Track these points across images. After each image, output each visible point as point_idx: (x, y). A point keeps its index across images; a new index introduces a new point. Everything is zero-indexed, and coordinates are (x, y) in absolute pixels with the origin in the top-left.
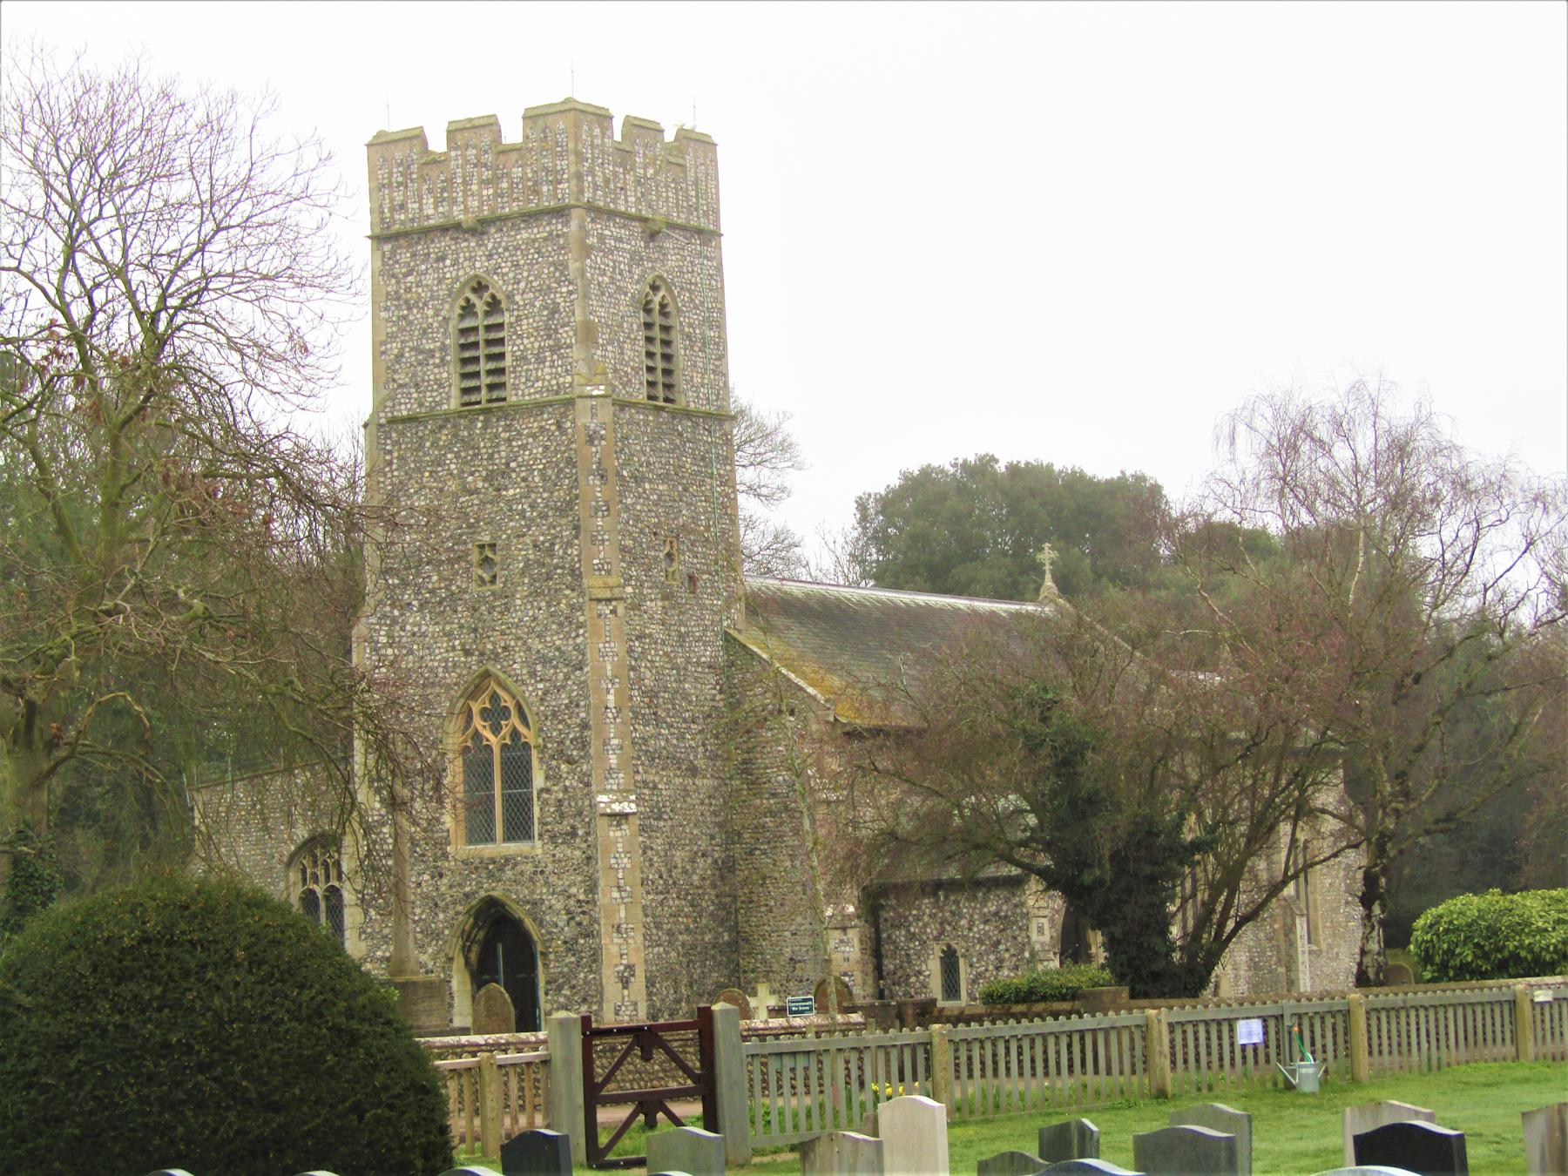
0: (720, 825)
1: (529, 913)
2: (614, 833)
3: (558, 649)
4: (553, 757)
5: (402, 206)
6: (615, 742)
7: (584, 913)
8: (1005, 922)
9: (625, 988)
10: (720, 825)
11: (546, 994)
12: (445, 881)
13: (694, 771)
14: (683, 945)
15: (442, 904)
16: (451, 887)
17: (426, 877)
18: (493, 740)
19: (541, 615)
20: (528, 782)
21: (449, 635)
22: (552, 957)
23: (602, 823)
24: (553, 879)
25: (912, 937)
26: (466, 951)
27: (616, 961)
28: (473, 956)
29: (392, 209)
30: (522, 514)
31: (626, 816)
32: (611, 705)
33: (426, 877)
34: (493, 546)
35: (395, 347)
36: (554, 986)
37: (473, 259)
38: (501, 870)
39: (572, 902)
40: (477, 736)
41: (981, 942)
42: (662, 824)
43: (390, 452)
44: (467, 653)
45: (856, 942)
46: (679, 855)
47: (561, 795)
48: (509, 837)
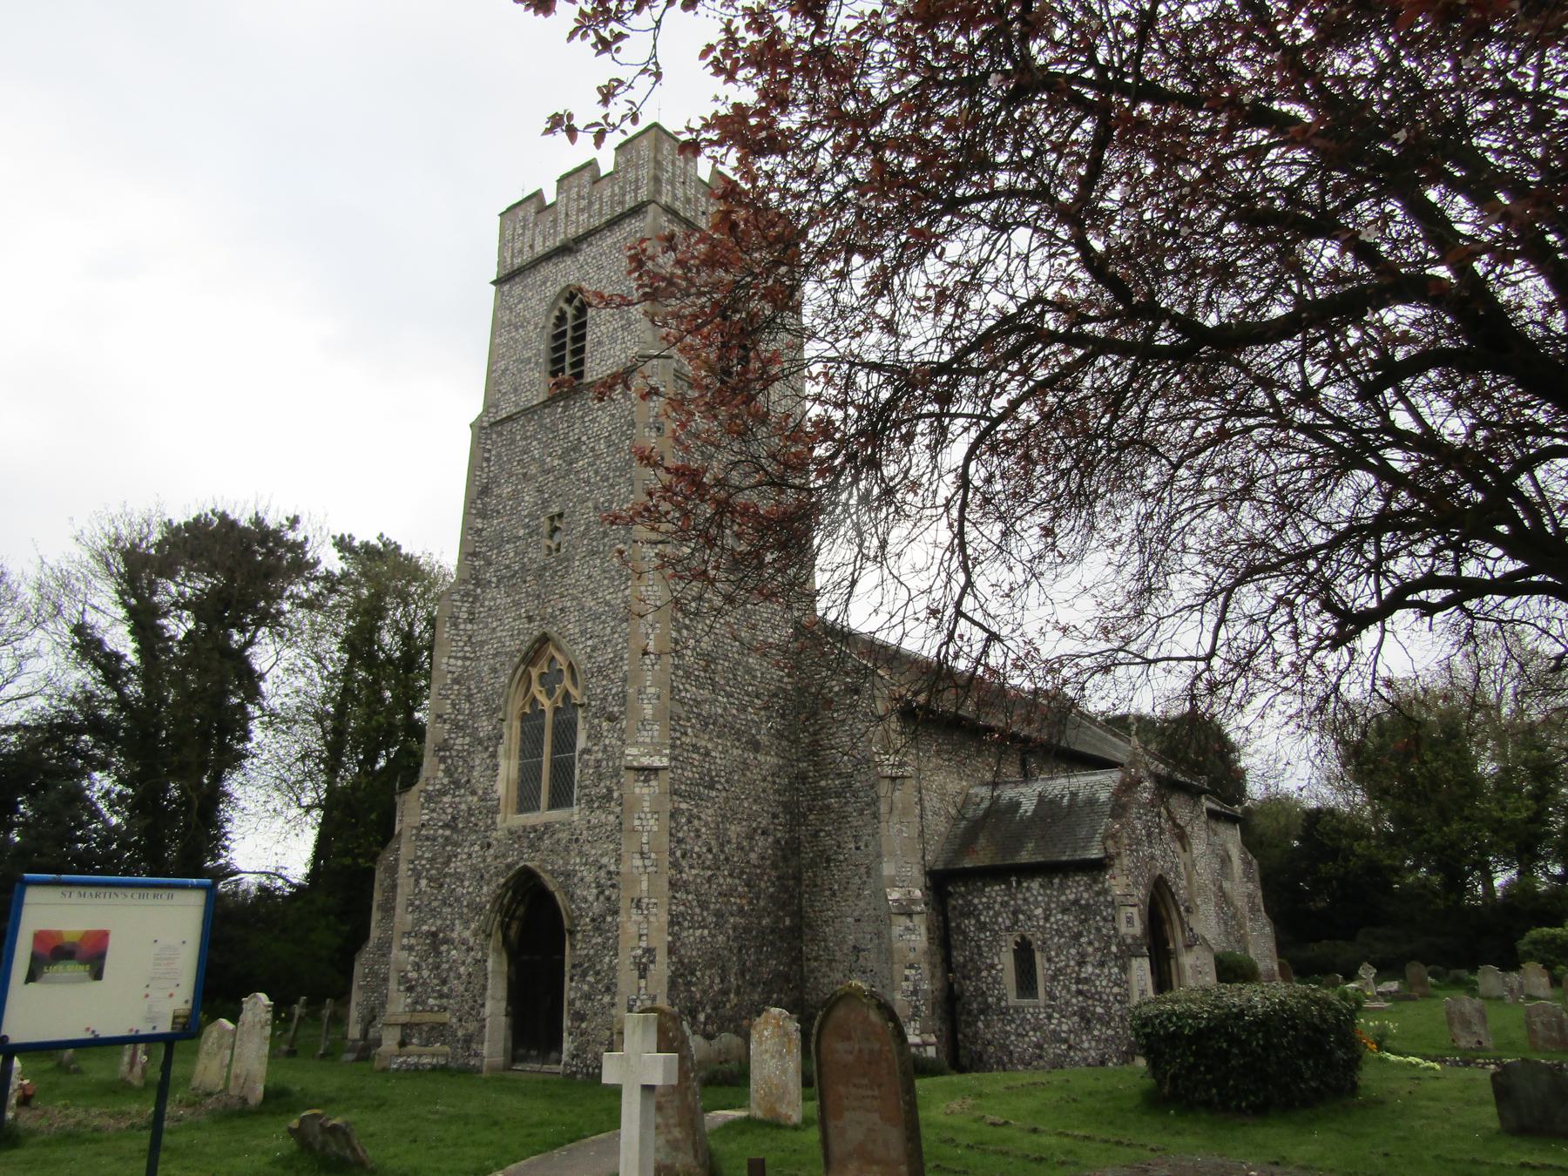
0: (784, 805)
1: (563, 886)
2: (640, 789)
3: (607, 603)
4: (595, 716)
5: (521, 251)
6: (652, 690)
7: (613, 886)
8: (1085, 911)
9: (642, 977)
10: (784, 805)
11: (571, 980)
12: (492, 851)
13: (756, 746)
14: (735, 929)
15: (487, 876)
16: (496, 857)
17: (477, 848)
18: (546, 703)
19: (596, 573)
20: (573, 747)
21: (517, 604)
22: (579, 936)
23: (628, 777)
24: (586, 847)
25: (982, 927)
26: (505, 928)
27: (634, 943)
28: (513, 932)
29: (513, 256)
30: (588, 482)
31: (655, 770)
32: (651, 648)
33: (477, 848)
34: (560, 515)
35: (502, 364)
36: (579, 970)
37: (567, 273)
38: (540, 839)
39: (603, 873)
40: (534, 700)
41: (1059, 933)
42: (714, 794)
43: (489, 451)
44: (530, 619)
45: (923, 930)
46: (734, 830)
47: (600, 755)
48: (553, 805)
